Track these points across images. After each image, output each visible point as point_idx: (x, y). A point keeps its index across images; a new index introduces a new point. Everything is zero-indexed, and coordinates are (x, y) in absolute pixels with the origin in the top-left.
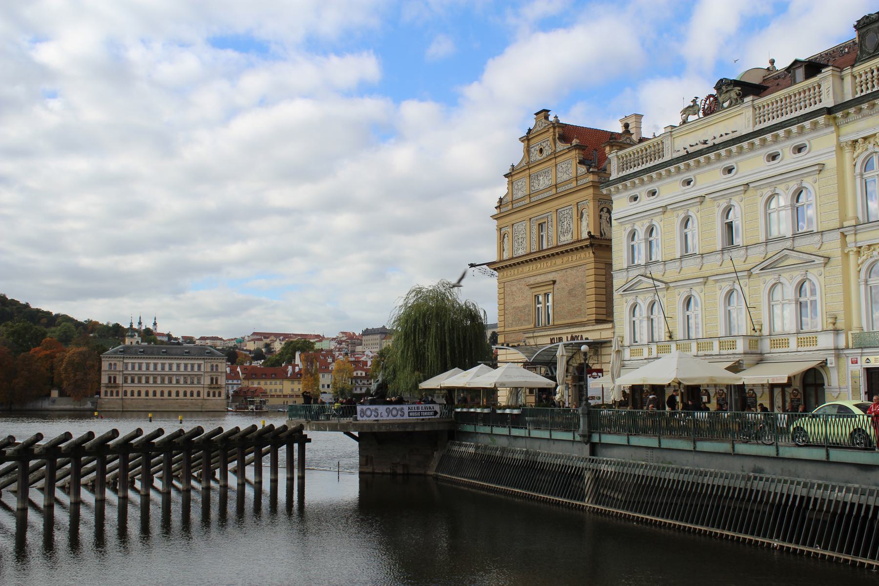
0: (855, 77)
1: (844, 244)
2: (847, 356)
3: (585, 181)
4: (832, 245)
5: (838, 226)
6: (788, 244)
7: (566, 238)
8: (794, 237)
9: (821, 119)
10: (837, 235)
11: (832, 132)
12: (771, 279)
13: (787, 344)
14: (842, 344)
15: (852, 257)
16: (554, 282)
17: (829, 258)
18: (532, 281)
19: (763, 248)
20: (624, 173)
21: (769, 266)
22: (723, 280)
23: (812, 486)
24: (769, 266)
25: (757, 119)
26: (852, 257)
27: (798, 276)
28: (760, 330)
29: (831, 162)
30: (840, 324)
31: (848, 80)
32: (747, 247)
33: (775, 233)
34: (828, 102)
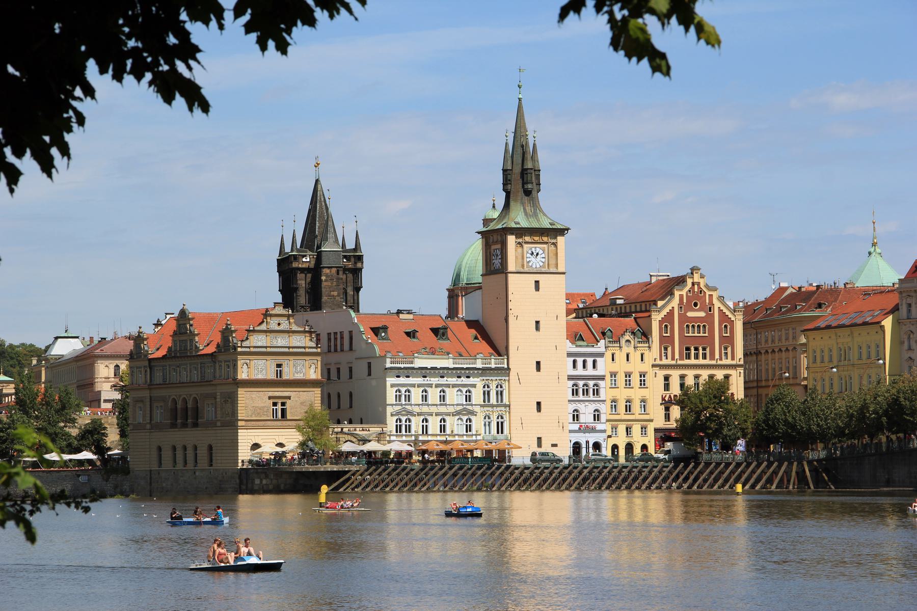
3: (315, 350)
4: (477, 409)
7: (299, 376)
16: (289, 398)
18: (271, 394)
20: (393, 365)
24: (458, 413)
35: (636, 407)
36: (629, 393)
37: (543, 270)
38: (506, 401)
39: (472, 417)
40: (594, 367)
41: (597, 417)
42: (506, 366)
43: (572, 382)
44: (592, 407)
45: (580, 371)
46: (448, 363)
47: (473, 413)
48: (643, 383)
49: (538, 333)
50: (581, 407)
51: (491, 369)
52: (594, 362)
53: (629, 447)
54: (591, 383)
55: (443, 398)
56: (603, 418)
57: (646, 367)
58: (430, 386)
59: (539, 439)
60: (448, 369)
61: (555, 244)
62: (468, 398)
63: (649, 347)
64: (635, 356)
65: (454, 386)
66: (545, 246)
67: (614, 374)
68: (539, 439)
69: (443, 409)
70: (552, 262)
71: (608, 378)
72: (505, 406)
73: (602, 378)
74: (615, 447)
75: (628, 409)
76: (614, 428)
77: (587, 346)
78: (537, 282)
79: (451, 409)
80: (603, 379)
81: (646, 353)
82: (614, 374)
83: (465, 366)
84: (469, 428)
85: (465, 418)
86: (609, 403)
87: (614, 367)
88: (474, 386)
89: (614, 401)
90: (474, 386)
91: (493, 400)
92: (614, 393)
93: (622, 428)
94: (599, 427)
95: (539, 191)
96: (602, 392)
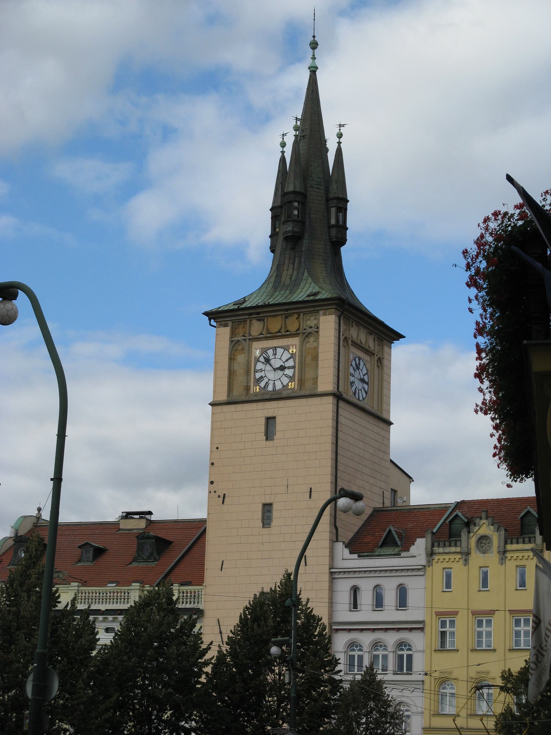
37: (285, 394)
42: (201, 606)
45: (367, 613)
49: (266, 531)
54: (391, 639)
66: (296, 341)
70: (309, 375)
73: (418, 627)
77: (398, 555)
78: (270, 421)
80: (422, 629)
87: (445, 602)
89: (443, 681)
92: (444, 662)
95: (343, 241)
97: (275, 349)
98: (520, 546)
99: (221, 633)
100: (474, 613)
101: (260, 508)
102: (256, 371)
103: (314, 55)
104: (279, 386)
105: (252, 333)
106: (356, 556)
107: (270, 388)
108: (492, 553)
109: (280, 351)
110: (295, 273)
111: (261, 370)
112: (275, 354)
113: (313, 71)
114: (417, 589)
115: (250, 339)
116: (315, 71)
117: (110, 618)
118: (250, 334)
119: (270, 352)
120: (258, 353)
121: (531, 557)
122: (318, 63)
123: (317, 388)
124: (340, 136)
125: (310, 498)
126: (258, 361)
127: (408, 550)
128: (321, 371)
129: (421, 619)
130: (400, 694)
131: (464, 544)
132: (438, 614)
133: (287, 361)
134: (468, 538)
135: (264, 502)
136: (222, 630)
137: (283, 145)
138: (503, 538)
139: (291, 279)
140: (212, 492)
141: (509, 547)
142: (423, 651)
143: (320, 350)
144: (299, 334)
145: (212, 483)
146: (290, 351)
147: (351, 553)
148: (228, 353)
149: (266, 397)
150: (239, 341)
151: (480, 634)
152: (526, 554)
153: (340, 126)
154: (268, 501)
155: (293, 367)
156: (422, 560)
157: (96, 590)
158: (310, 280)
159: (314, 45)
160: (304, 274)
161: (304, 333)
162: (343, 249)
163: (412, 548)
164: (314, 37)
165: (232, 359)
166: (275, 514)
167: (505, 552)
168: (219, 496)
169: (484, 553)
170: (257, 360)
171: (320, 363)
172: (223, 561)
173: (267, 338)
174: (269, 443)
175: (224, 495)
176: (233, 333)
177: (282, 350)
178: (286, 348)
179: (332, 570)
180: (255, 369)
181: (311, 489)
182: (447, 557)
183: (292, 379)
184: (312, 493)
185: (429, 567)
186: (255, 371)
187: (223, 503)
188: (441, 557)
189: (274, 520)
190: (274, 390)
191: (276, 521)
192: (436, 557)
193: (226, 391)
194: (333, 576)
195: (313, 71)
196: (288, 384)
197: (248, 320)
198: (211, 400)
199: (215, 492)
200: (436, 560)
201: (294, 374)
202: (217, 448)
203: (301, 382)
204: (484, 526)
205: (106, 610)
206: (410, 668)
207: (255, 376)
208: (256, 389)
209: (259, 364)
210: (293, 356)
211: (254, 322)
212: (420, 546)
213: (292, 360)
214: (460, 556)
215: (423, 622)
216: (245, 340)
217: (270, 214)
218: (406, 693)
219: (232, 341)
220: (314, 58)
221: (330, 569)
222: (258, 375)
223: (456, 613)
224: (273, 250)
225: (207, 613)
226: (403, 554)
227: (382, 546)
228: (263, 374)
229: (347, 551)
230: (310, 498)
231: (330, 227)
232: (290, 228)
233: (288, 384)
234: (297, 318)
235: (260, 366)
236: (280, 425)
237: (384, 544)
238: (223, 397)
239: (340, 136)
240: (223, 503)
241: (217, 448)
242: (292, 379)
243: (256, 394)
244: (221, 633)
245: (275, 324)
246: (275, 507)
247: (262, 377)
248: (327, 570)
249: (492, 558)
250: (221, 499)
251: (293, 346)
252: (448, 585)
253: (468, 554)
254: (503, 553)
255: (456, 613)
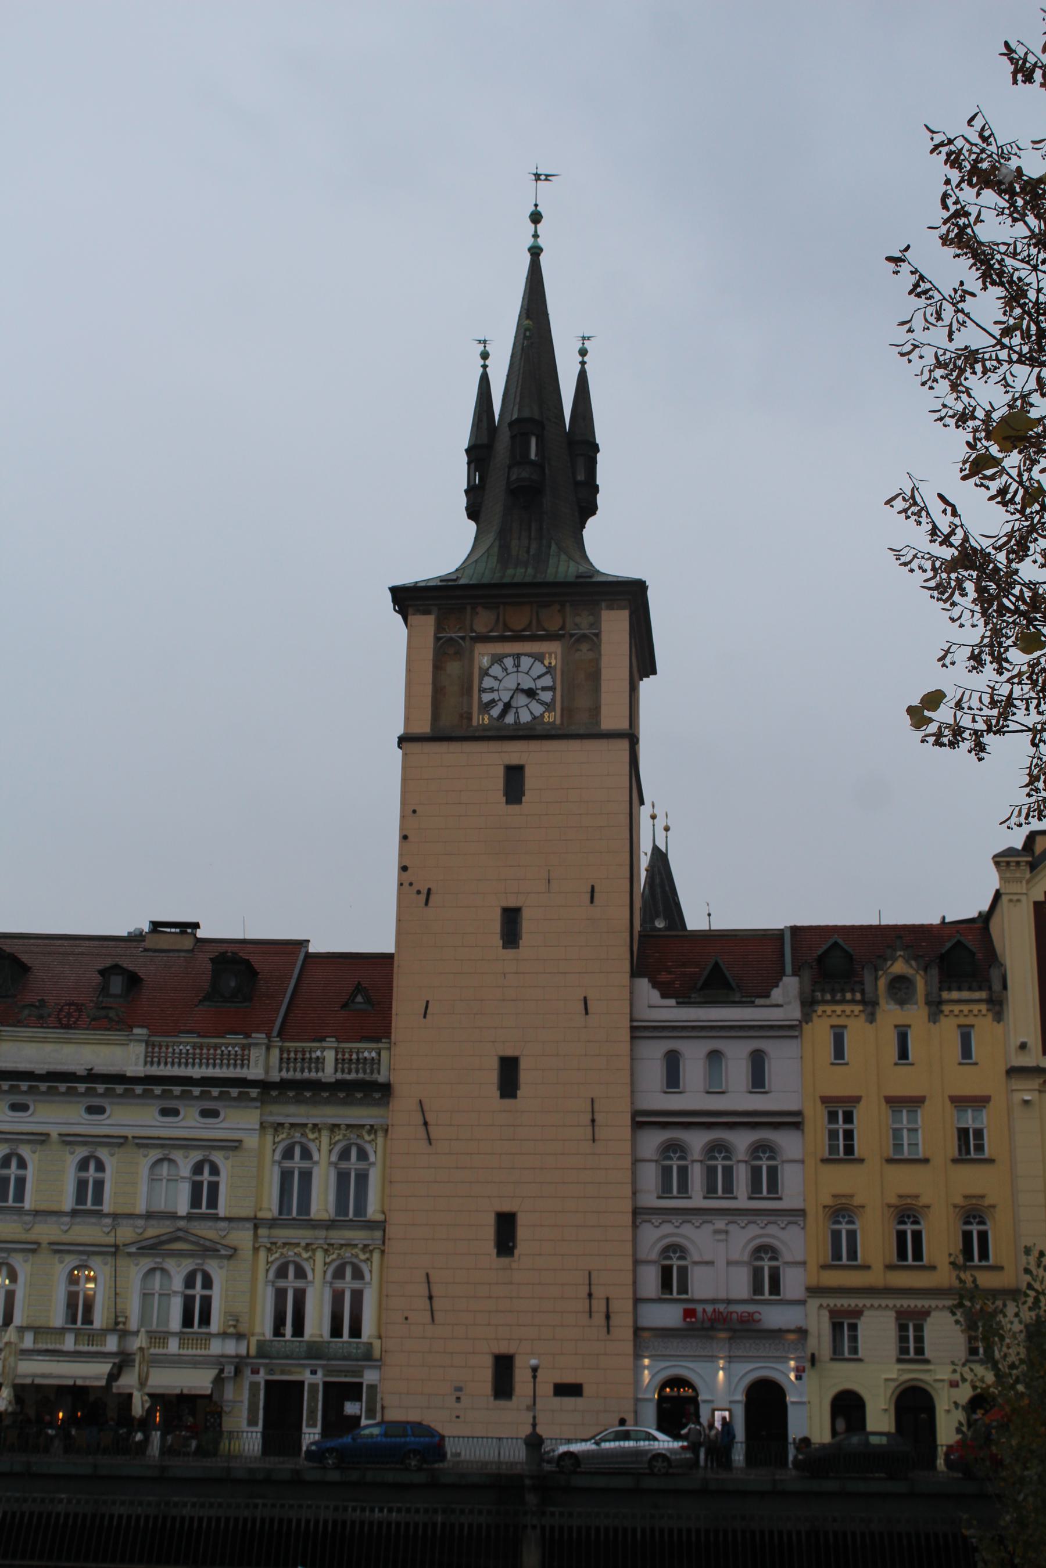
0: (282, 1051)
1: (256, 1236)
2: (247, 1364)
4: (242, 1238)
5: (251, 1215)
6: (182, 1224)
8: (189, 1217)
9: (254, 1092)
10: (250, 1225)
11: (257, 1108)
12: (147, 1263)
13: (165, 1345)
14: (243, 1351)
15: (262, 1254)
17: (235, 1249)
19: (141, 1222)
21: (152, 1248)
22: (69, 1252)
23: (345, 1509)
24: (152, 1248)
25: (149, 1060)
26: (262, 1254)
27: (188, 1265)
28: (124, 1323)
29: (251, 1141)
30: (243, 1328)
31: (275, 1053)
32: (115, 1216)
33: (161, 1206)
34: (255, 1072)
35: (940, 1240)
36: (904, 1181)
37: (539, 730)
38: (373, 1211)
39: (213, 1267)
40: (758, 1080)
41: (768, 1282)
42: (381, 1079)
43: (652, 1141)
44: (743, 1238)
45: (693, 1097)
46: (125, 1056)
47: (209, 1250)
48: (969, 1145)
49: (510, 953)
50: (699, 1239)
51: (317, 1086)
52: (758, 1062)
53: (914, 1405)
54: (741, 1141)
55: (89, 1193)
56: (793, 1283)
57: (984, 1077)
58: (41, 1139)
59: (503, 1367)
60: (121, 1079)
61: (593, 640)
62: (204, 1195)
63: (997, 1005)
64: (934, 1040)
65: (143, 1143)
67: (841, 1110)
68: (503, 1367)
69: (87, 1232)
71: (816, 1118)
72: (372, 1225)
73: (792, 1121)
74: (848, 1407)
75: (908, 1248)
76: (845, 1326)
79: (126, 1233)
80: (798, 1126)
81: (984, 1028)
82: (841, 1110)
83: (196, 1072)
84: (196, 1313)
85: (178, 1271)
86: (818, 1226)
87: (839, 1083)
88: (234, 1146)
89: (842, 1211)
90: (234, 1146)
91: (322, 1202)
92: (841, 1180)
93: (877, 1330)
94: (774, 1317)
96: (791, 1179)
97: (517, 656)
98: (965, 995)
99: (426, 1124)
100: (890, 1100)
101: (497, 916)
102: (482, 690)
103: (536, 231)
104: (525, 717)
105: (475, 627)
106: (672, 1002)
107: (510, 719)
108: (916, 1003)
109: (526, 662)
110: (534, 547)
111: (492, 690)
112: (518, 666)
113: (535, 252)
114: (782, 1058)
115: (472, 638)
116: (539, 255)
117: (215, 1092)
118: (472, 631)
119: (509, 662)
120: (485, 661)
121: (984, 1012)
122: (541, 242)
123: (598, 723)
124: (583, 352)
125: (592, 901)
126: (487, 674)
127: (767, 996)
128: (605, 698)
129: (794, 1107)
130: (761, 1232)
131: (868, 987)
132: (825, 1100)
133: (539, 677)
134: (876, 979)
135: (505, 904)
136: (428, 1120)
137: (485, 356)
138: (936, 980)
139: (528, 552)
140: (406, 884)
141: (945, 995)
142: (803, 1162)
143: (605, 662)
144: (563, 636)
145: (404, 869)
146: (546, 663)
147: (664, 996)
148: (430, 655)
149: (504, 733)
150: (451, 639)
151: (897, 1133)
152: (975, 1008)
153: (584, 338)
154: (512, 903)
155: (552, 689)
156: (794, 1012)
157: (160, 1042)
158: (563, 557)
159: (536, 218)
160: (550, 547)
161: (572, 635)
162: (591, 522)
163: (777, 995)
164: (536, 205)
165: (438, 667)
166: (527, 925)
167: (941, 1002)
168: (419, 892)
169: (902, 1003)
170: (485, 673)
171: (605, 686)
172: (428, 1002)
173: (502, 639)
174: (514, 808)
175: (429, 890)
176: (439, 627)
177: (531, 660)
178: (539, 658)
179: (635, 1024)
180: (480, 687)
181: (593, 887)
182: (839, 1009)
183: (549, 706)
184: (596, 895)
185: (807, 1023)
186: (480, 691)
187: (427, 903)
188: (829, 1009)
189: (525, 936)
190: (517, 722)
191: (525, 940)
192: (820, 1009)
193: (429, 717)
194: (638, 1031)
195: (535, 252)
196: (542, 715)
197: (469, 608)
198: (400, 731)
199: (411, 884)
200: (819, 1012)
201: (553, 699)
202: (414, 812)
203: (568, 712)
204: (900, 959)
205: (203, 1078)
206: (773, 1186)
207: (480, 698)
208: (483, 719)
209: (486, 679)
210: (550, 670)
211: (480, 610)
212: (789, 987)
213: (548, 677)
214: (861, 1008)
215: (799, 1113)
216: (463, 638)
217: (464, 458)
218: (772, 1229)
219: (437, 639)
220: (536, 236)
221: (632, 1020)
222: (486, 697)
223: (857, 1099)
224: (473, 513)
225: (398, 1089)
226: (759, 1001)
227: (702, 988)
228: (495, 696)
229: (655, 996)
230: (592, 901)
231: (577, 484)
232: (524, 475)
233: (542, 715)
234: (559, 611)
235: (488, 683)
236: (531, 782)
237: (706, 985)
238: (424, 727)
239: (583, 352)
240: (427, 903)
241: (414, 812)
242: (549, 706)
243: (485, 728)
244: (426, 1124)
245: (519, 619)
246: (526, 914)
247: (493, 701)
248: (627, 1024)
249: (915, 1015)
250: (423, 897)
251: (550, 654)
252: (839, 1052)
253: (875, 1004)
254: (935, 1008)
255: (857, 1099)
